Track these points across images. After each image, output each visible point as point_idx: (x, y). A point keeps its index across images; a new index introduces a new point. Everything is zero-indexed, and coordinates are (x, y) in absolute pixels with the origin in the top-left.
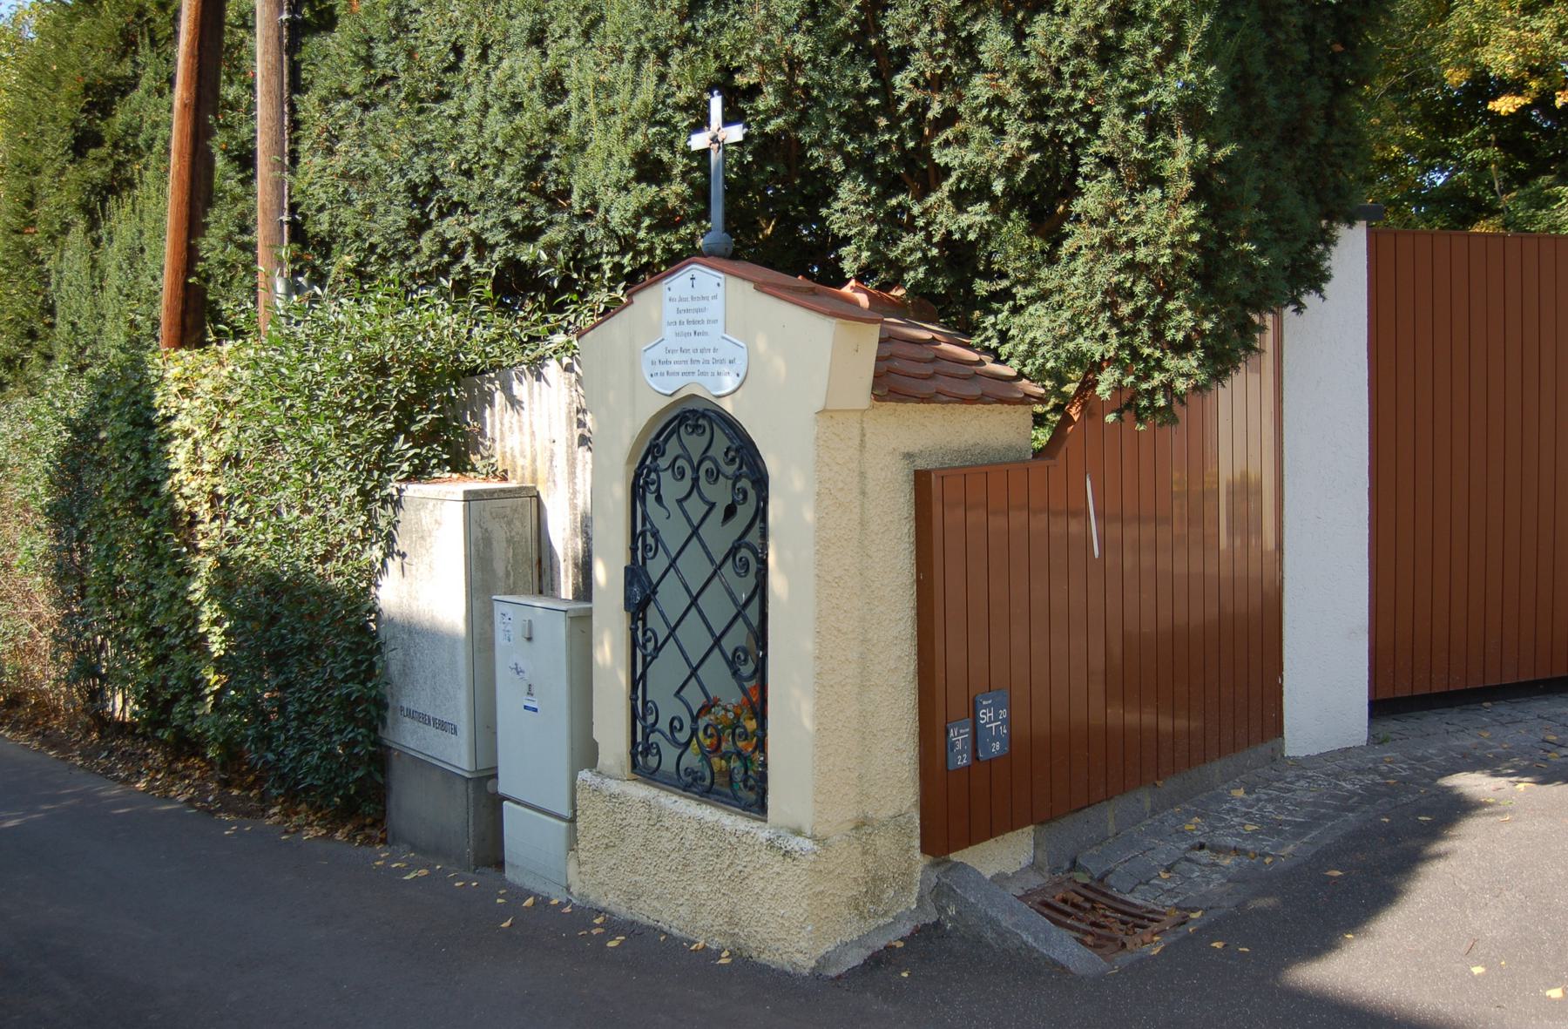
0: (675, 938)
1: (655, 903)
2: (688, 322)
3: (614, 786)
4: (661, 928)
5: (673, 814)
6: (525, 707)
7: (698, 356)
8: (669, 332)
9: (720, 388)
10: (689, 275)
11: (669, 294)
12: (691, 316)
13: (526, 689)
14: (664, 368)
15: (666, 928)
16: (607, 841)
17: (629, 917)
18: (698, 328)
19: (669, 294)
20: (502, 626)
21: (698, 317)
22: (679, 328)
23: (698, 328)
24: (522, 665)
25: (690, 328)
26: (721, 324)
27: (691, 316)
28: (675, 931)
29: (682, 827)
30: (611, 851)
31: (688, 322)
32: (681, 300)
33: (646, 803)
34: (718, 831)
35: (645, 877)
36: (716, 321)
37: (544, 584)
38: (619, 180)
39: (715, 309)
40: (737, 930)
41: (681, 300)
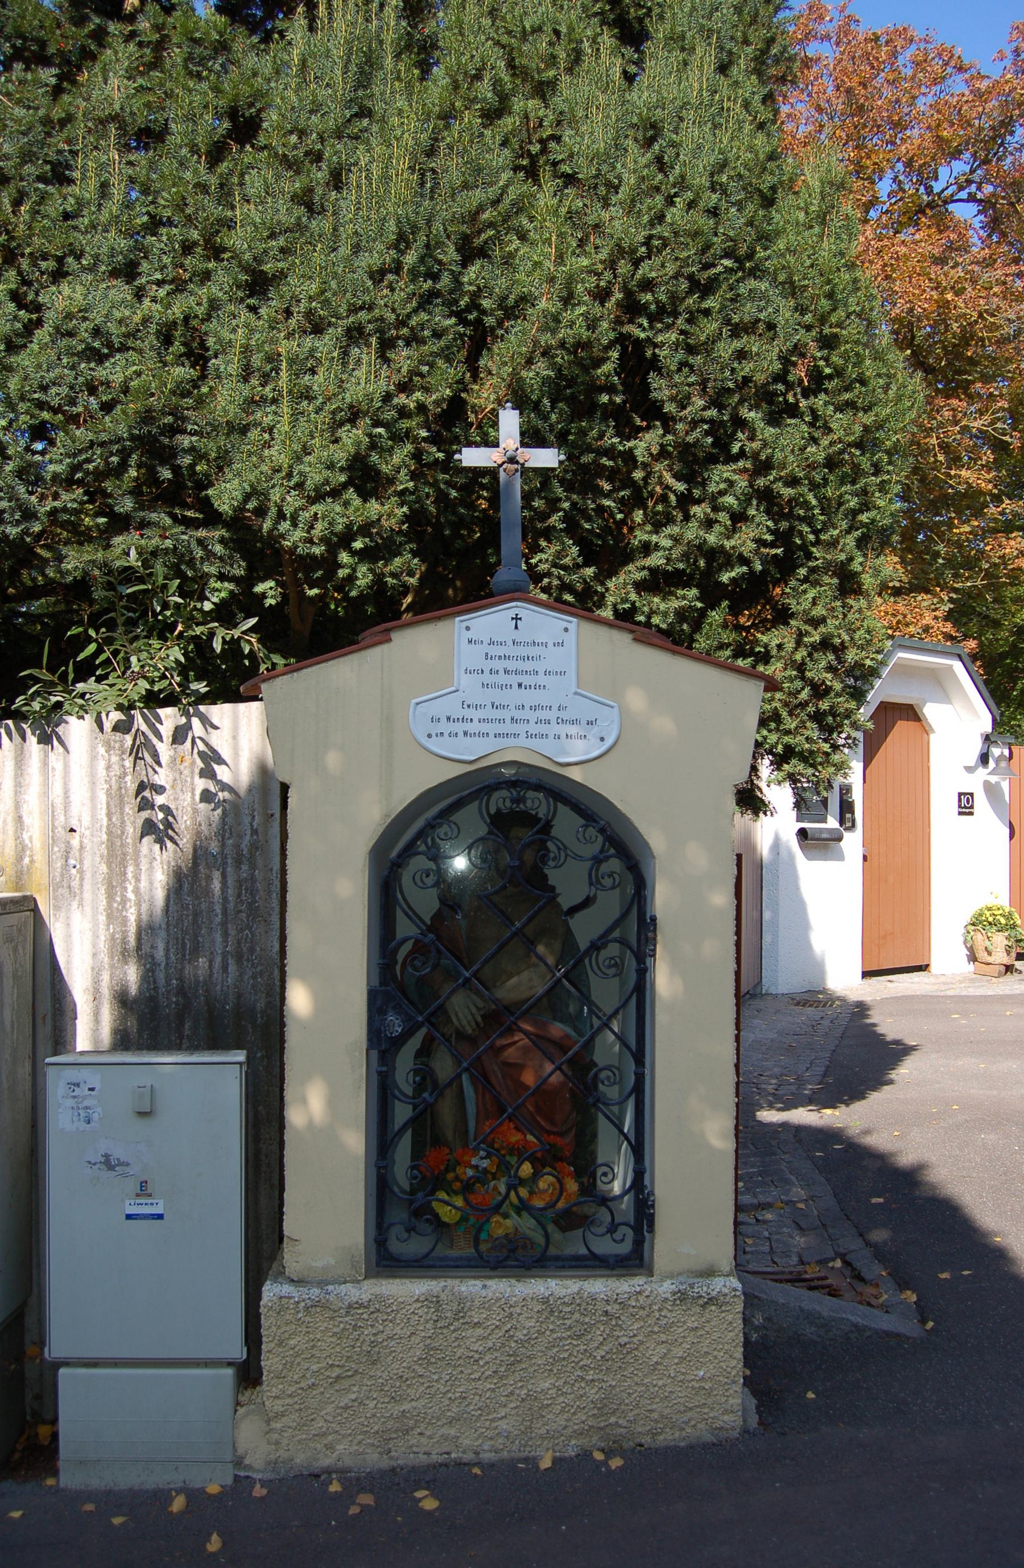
0: (492, 1465)
1: (445, 1431)
2: (506, 672)
3: (352, 1292)
4: (455, 1460)
5: (486, 1305)
6: (129, 1217)
7: (519, 715)
8: (465, 681)
9: (566, 753)
10: (512, 613)
11: (469, 635)
12: (511, 665)
13: (133, 1186)
14: (459, 728)
15: (469, 1457)
16: (337, 1371)
17: (385, 1463)
18: (526, 680)
19: (469, 635)
20: (70, 1102)
21: (528, 666)
22: (487, 678)
23: (526, 680)
24: (118, 1153)
25: (513, 680)
26: (572, 675)
27: (511, 665)
28: (487, 1456)
29: (511, 1314)
30: (345, 1384)
31: (506, 672)
32: (492, 643)
33: (435, 1302)
34: (583, 1304)
35: (422, 1402)
36: (563, 673)
37: (40, 1036)
38: (327, 482)
39: (564, 658)
40: (613, 1420)
41: (492, 643)
